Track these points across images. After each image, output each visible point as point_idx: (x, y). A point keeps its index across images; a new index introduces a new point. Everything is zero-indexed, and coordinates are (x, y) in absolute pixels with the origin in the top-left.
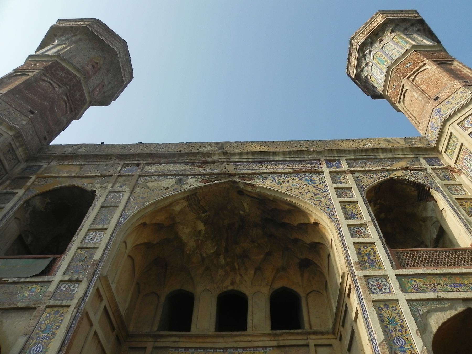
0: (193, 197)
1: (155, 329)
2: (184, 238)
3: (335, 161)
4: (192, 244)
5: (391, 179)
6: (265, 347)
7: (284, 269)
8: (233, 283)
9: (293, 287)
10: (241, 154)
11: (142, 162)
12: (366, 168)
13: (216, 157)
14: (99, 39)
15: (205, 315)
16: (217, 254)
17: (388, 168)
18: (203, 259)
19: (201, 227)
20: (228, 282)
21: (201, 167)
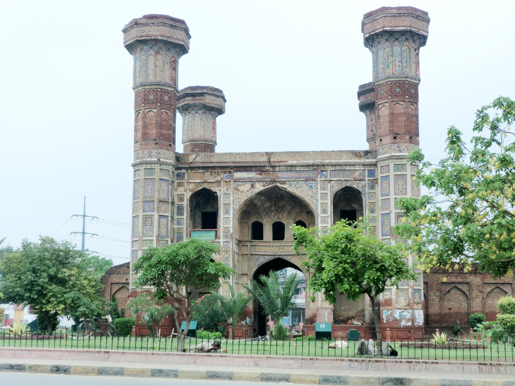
0: (260, 194)
1: (250, 239)
2: (256, 203)
3: (324, 171)
4: (260, 203)
5: (347, 186)
7: (300, 213)
8: (278, 218)
9: (303, 221)
10: (279, 166)
11: (232, 171)
12: (338, 179)
13: (268, 168)
14: (171, 43)
15: (268, 232)
16: (271, 206)
17: (348, 179)
18: (265, 209)
19: (263, 198)
20: (276, 218)
21: (260, 174)
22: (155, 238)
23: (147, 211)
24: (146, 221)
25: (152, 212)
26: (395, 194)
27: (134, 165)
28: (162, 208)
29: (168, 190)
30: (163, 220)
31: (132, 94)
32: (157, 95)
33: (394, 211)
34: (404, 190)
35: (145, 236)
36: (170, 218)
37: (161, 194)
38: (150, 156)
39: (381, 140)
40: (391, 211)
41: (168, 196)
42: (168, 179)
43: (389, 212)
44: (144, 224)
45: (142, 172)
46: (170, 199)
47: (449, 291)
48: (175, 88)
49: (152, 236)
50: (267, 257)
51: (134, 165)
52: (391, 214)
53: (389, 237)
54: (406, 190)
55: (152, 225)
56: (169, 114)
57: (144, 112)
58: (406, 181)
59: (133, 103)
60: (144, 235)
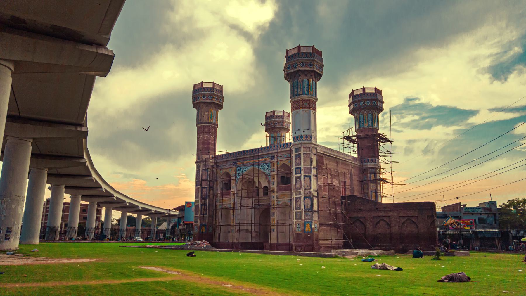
47: (379, 222)
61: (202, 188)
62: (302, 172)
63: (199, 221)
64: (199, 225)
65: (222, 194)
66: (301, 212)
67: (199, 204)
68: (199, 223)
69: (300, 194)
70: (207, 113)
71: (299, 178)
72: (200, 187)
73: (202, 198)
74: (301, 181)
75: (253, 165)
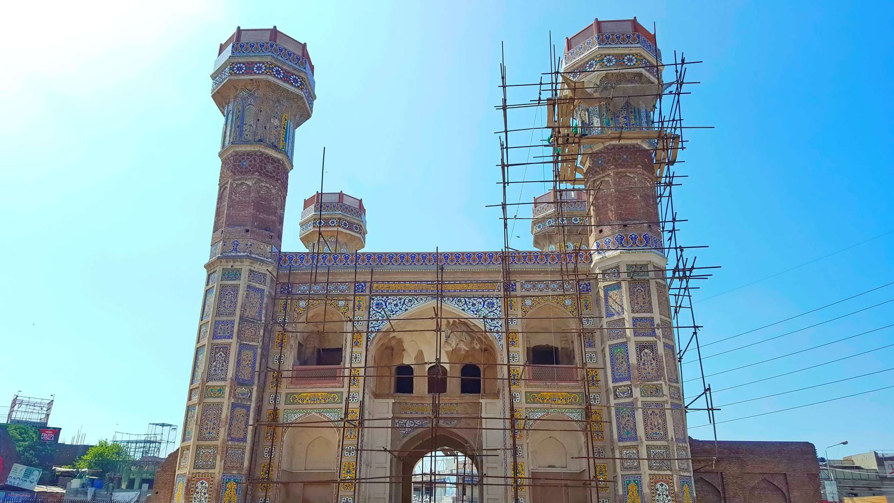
6: (457, 404)
22: (228, 383)
23: (221, 338)
24: (216, 353)
25: (229, 338)
26: (633, 312)
27: (207, 266)
28: (247, 332)
29: (261, 305)
30: (247, 354)
31: (219, 163)
32: (255, 161)
33: (634, 339)
34: (647, 306)
35: (211, 380)
36: (259, 351)
37: (248, 310)
38: (236, 250)
39: (601, 231)
40: (628, 339)
41: (260, 315)
42: (261, 287)
43: (624, 340)
44: (212, 359)
45: (217, 276)
46: (263, 318)
48: (286, 154)
49: (224, 379)
50: (417, 422)
51: (207, 266)
52: (629, 344)
53: (628, 383)
54: (651, 304)
55: (226, 361)
56: (274, 191)
57: (232, 184)
58: (649, 290)
59: (219, 175)
60: (209, 377)
61: (242, 347)
62: (659, 332)
63: (219, 464)
64: (218, 478)
65: (299, 378)
66: (666, 447)
67: (226, 402)
68: (217, 471)
69: (658, 391)
70: (276, 122)
71: (652, 347)
72: (234, 341)
73: (238, 382)
74: (656, 358)
75: (440, 295)
